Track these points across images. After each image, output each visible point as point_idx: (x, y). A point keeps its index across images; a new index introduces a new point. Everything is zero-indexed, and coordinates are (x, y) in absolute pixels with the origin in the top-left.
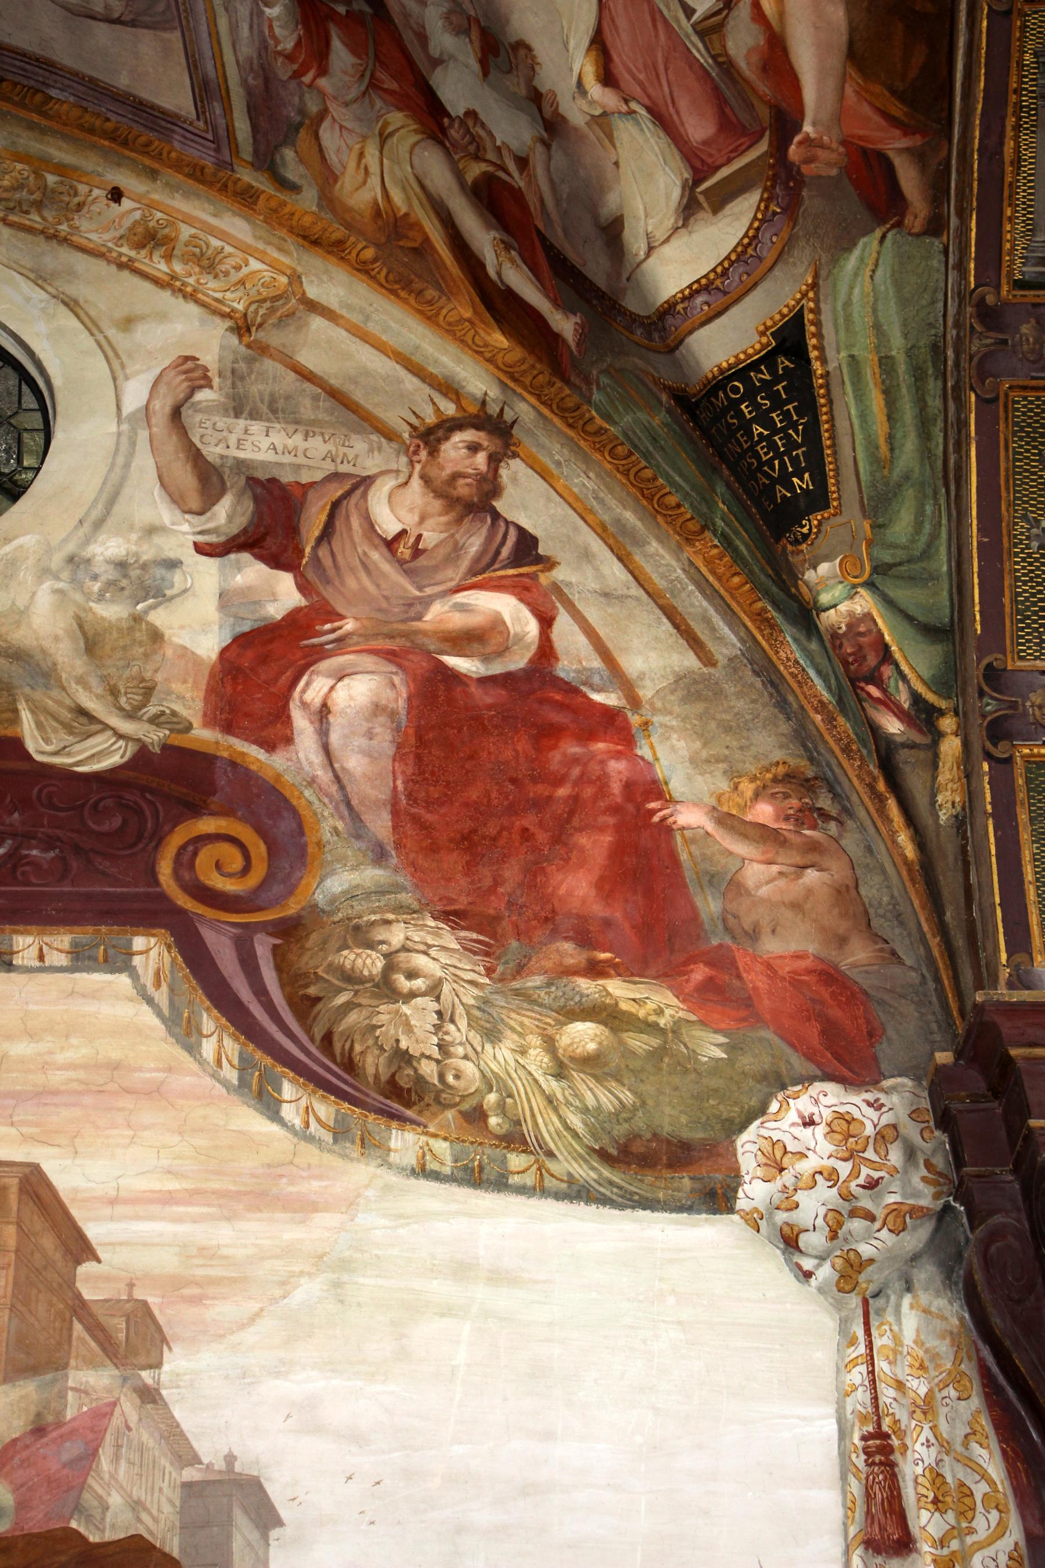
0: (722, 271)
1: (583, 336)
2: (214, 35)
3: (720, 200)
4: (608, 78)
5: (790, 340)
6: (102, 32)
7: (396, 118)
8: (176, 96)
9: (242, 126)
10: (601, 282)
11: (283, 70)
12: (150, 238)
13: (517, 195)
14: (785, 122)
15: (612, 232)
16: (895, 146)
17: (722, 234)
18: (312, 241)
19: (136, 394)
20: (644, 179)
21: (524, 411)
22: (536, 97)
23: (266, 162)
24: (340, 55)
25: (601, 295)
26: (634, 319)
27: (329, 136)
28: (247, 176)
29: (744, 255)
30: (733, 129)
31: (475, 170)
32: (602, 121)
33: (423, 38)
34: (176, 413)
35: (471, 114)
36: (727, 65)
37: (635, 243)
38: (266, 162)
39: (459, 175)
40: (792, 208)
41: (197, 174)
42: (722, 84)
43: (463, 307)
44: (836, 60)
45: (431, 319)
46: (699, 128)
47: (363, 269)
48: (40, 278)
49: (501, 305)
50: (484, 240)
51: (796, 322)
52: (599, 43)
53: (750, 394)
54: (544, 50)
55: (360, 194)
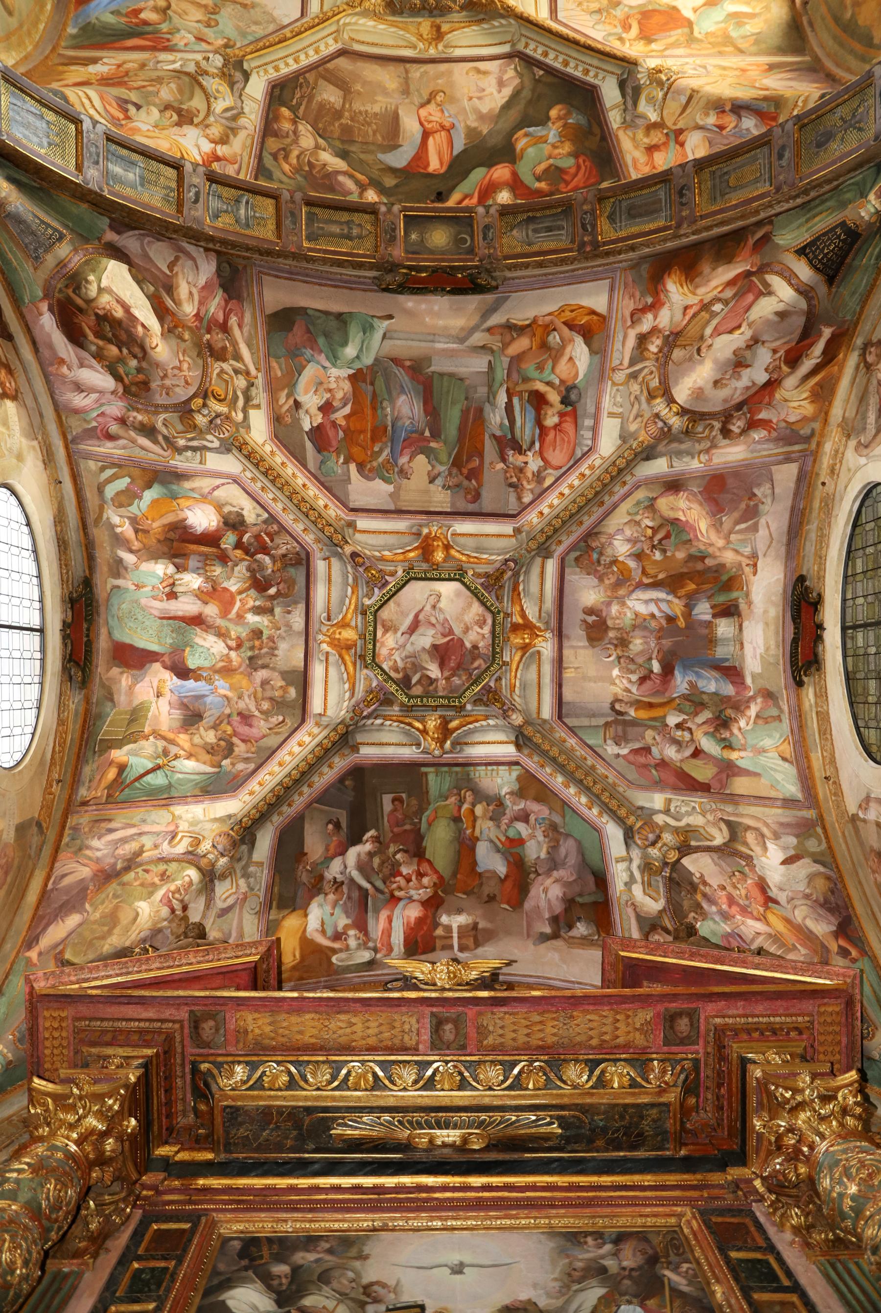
0: (784, 278)
1: (829, 325)
2: (769, 456)
3: (767, 285)
4: (739, 327)
5: (801, 252)
6: (777, 491)
7: (777, 396)
8: (793, 469)
9: (797, 448)
10: (803, 319)
11: (774, 434)
12: (832, 471)
13: (787, 352)
14: (748, 274)
15: (782, 315)
16: (751, 242)
17: (777, 282)
18: (826, 421)
19: (863, 461)
20: (764, 309)
21: (859, 341)
22: (749, 347)
23: (807, 439)
24: (763, 415)
25: (808, 320)
26: (809, 305)
27: (792, 419)
28: (813, 446)
29: (780, 274)
30: (750, 288)
31: (785, 369)
32: (750, 325)
33: (748, 388)
34: (866, 447)
35: (766, 370)
36: (735, 295)
37: (781, 307)
38: (807, 439)
39: (790, 374)
40: (768, 265)
41: (815, 461)
42: (739, 295)
43: (833, 369)
44: (731, 266)
45: (838, 379)
46: (750, 297)
47: (830, 403)
48: (842, 499)
49: (829, 356)
50: (807, 365)
51: (797, 252)
52: (730, 332)
53: (816, 257)
54: (734, 347)
55: (808, 409)
